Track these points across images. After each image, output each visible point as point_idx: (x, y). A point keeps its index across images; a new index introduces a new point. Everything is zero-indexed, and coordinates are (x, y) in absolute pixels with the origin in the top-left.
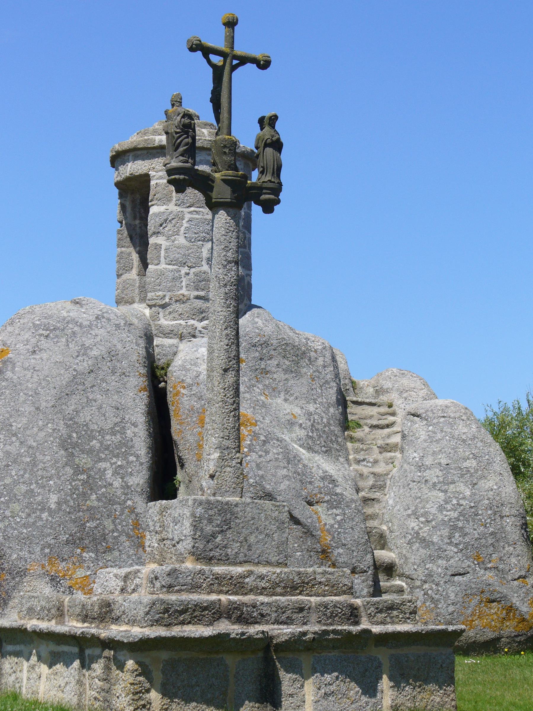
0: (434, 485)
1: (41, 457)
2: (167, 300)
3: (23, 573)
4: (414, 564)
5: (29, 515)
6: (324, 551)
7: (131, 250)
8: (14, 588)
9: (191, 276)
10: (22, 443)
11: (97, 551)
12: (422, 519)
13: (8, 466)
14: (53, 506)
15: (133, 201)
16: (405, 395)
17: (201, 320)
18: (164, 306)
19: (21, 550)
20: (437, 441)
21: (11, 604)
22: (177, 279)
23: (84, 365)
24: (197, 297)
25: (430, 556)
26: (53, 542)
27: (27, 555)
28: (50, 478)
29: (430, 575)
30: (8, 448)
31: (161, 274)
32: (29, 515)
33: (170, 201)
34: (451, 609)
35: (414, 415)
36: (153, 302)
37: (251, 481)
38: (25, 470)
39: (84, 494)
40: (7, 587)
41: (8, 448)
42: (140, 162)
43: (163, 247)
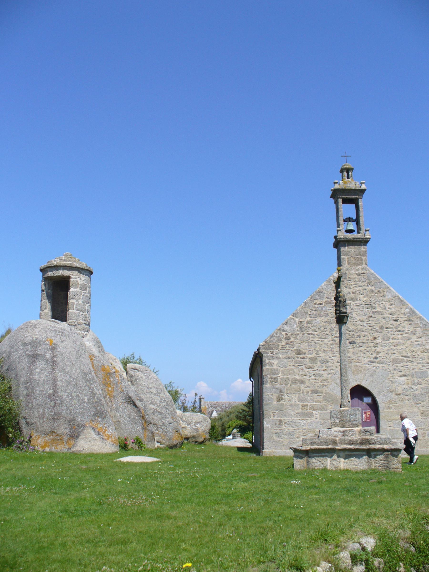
0: (155, 394)
1: (79, 383)
2: (76, 323)
3: (84, 426)
4: (157, 420)
5: (80, 405)
6: (143, 417)
7: (47, 301)
8: (81, 432)
9: (83, 315)
10: (70, 377)
11: (102, 418)
12: (156, 405)
13: (67, 385)
14: (87, 401)
15: (49, 283)
16: (114, 361)
17: (85, 332)
18: (74, 326)
19: (81, 417)
20: (151, 379)
21: (80, 437)
22: (79, 316)
23: (77, 348)
24: (85, 324)
25: (163, 418)
26: (90, 414)
27: (84, 420)
28: (83, 391)
29: (163, 424)
30: (66, 378)
31: (75, 313)
32: (80, 405)
33: (78, 287)
34: (170, 434)
35: (134, 369)
36: (71, 324)
37: (125, 392)
38: (74, 387)
39: (93, 397)
40: (78, 431)
41: (66, 378)
42: (66, 271)
43: (75, 304)
